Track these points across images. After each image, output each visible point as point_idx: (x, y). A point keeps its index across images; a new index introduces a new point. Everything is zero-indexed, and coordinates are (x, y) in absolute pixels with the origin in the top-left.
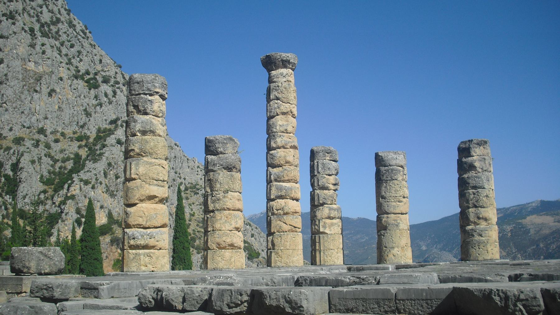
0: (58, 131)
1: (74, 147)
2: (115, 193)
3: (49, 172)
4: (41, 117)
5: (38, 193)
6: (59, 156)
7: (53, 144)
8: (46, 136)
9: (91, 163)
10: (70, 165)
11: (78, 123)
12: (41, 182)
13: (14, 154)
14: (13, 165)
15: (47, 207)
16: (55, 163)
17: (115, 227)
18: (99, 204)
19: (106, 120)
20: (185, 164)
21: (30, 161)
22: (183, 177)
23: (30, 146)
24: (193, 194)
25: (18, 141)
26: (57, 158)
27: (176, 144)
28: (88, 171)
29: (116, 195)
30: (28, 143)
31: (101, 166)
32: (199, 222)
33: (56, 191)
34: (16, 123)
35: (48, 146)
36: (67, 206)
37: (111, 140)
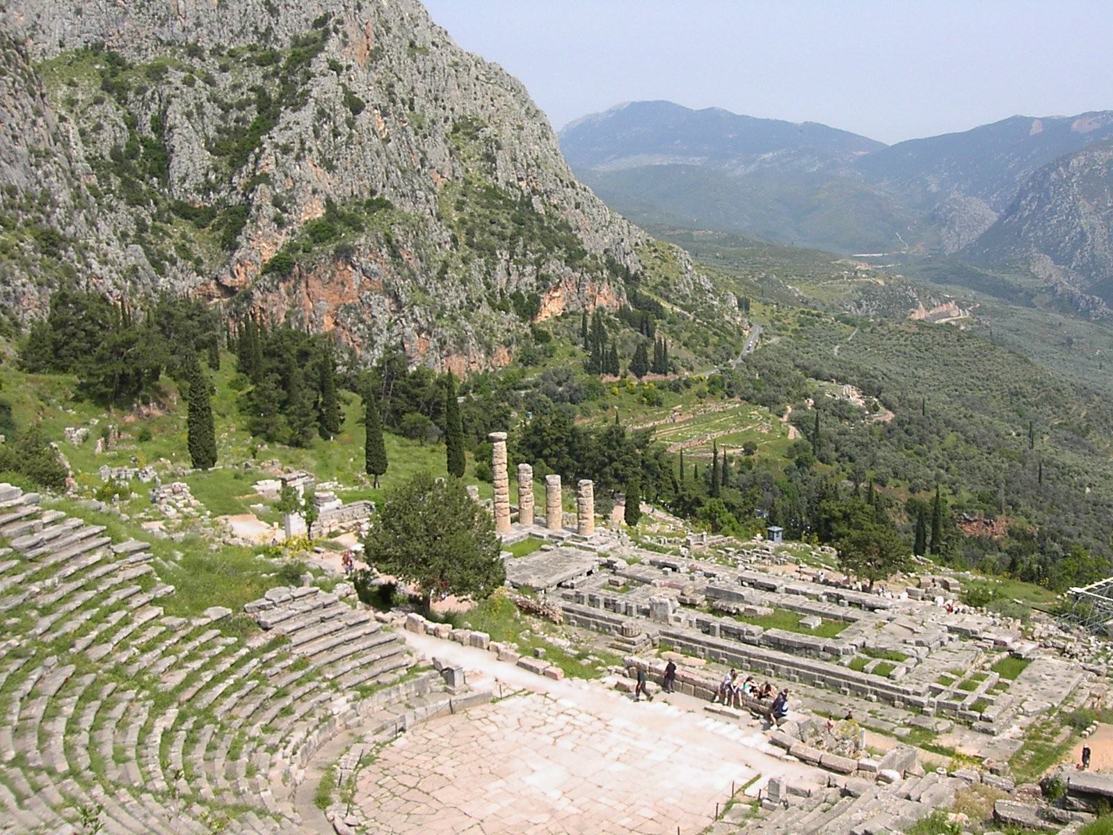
0: (223, 48)
1: (256, 76)
2: (335, 162)
3: (219, 130)
4: (189, 23)
5: (203, 171)
6: (231, 98)
7: (216, 75)
8: (204, 60)
9: (288, 111)
10: (252, 115)
11: (256, 28)
12: (208, 150)
13: (153, 99)
14: (154, 119)
15: (223, 194)
16: (227, 112)
17: (339, 226)
18: (310, 188)
19: (307, 20)
20: (452, 82)
21: (184, 113)
22: (449, 106)
23: (179, 84)
24: (467, 138)
25: (156, 73)
26: (229, 101)
27: (433, 43)
28: (285, 128)
29: (336, 167)
30: (176, 77)
31: (307, 115)
32: (480, 195)
33: (235, 165)
34: (147, 37)
35: (209, 81)
36: (258, 194)
37: (319, 64)
